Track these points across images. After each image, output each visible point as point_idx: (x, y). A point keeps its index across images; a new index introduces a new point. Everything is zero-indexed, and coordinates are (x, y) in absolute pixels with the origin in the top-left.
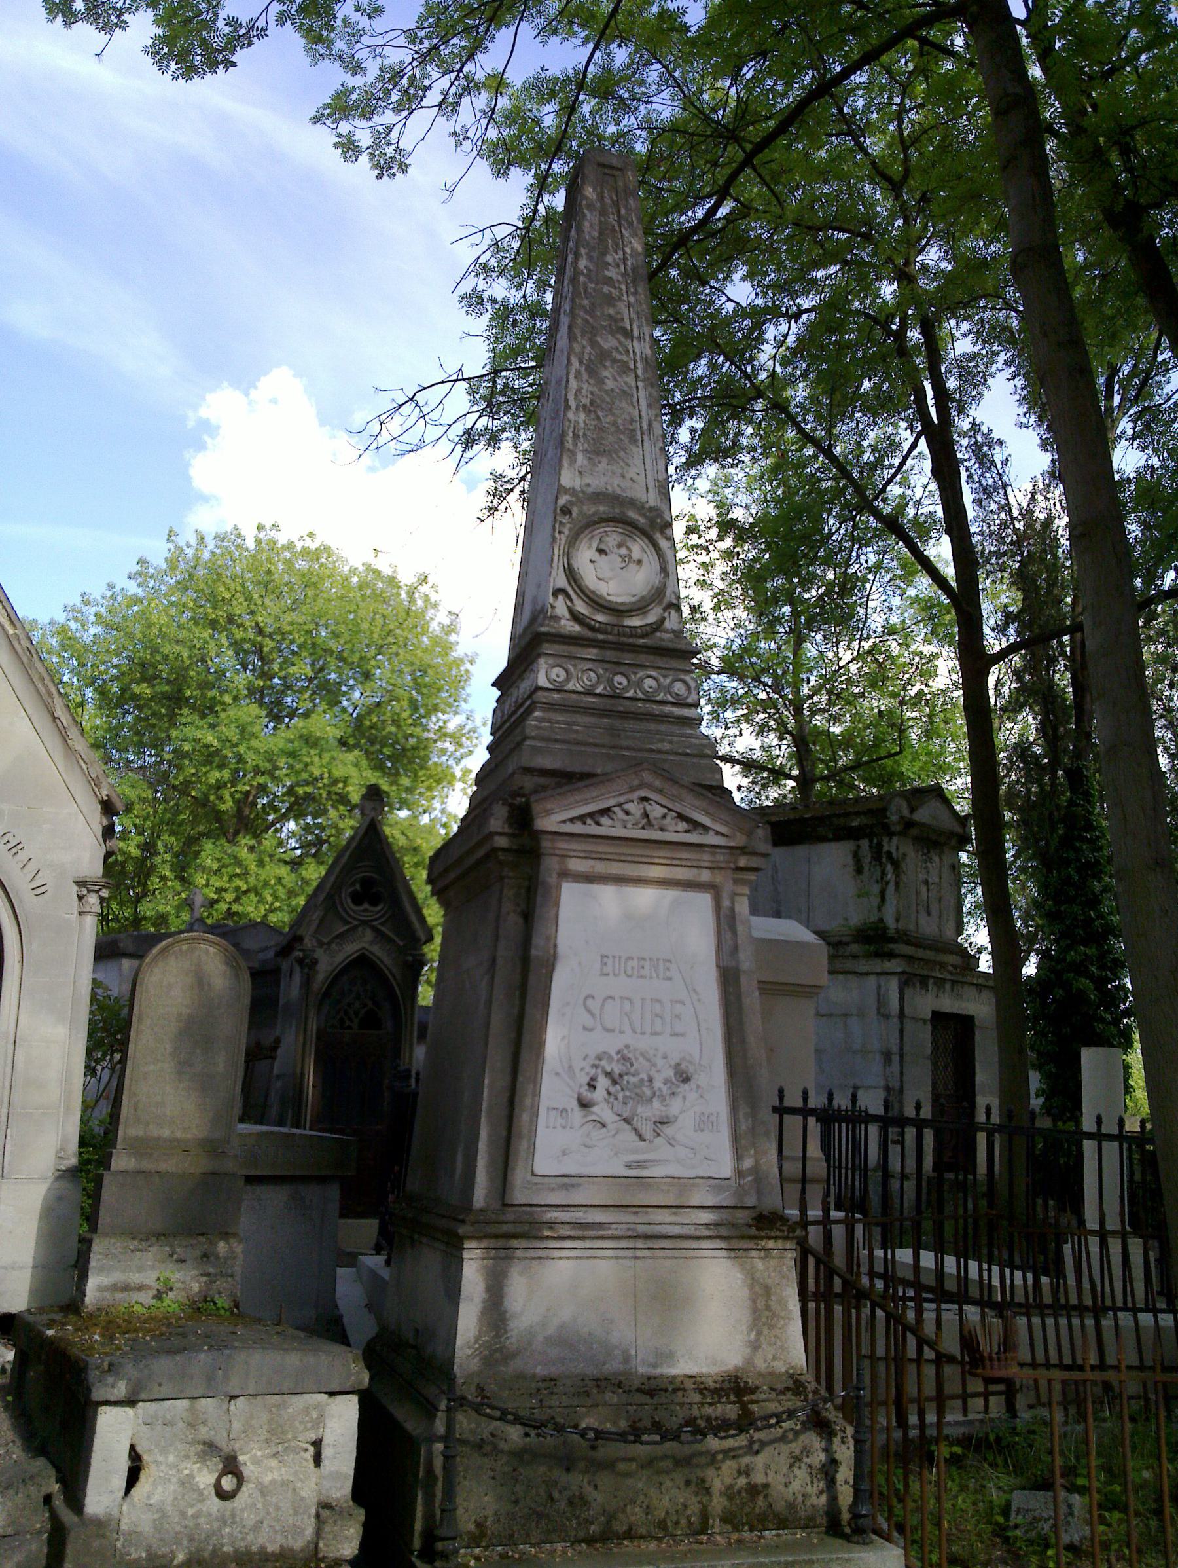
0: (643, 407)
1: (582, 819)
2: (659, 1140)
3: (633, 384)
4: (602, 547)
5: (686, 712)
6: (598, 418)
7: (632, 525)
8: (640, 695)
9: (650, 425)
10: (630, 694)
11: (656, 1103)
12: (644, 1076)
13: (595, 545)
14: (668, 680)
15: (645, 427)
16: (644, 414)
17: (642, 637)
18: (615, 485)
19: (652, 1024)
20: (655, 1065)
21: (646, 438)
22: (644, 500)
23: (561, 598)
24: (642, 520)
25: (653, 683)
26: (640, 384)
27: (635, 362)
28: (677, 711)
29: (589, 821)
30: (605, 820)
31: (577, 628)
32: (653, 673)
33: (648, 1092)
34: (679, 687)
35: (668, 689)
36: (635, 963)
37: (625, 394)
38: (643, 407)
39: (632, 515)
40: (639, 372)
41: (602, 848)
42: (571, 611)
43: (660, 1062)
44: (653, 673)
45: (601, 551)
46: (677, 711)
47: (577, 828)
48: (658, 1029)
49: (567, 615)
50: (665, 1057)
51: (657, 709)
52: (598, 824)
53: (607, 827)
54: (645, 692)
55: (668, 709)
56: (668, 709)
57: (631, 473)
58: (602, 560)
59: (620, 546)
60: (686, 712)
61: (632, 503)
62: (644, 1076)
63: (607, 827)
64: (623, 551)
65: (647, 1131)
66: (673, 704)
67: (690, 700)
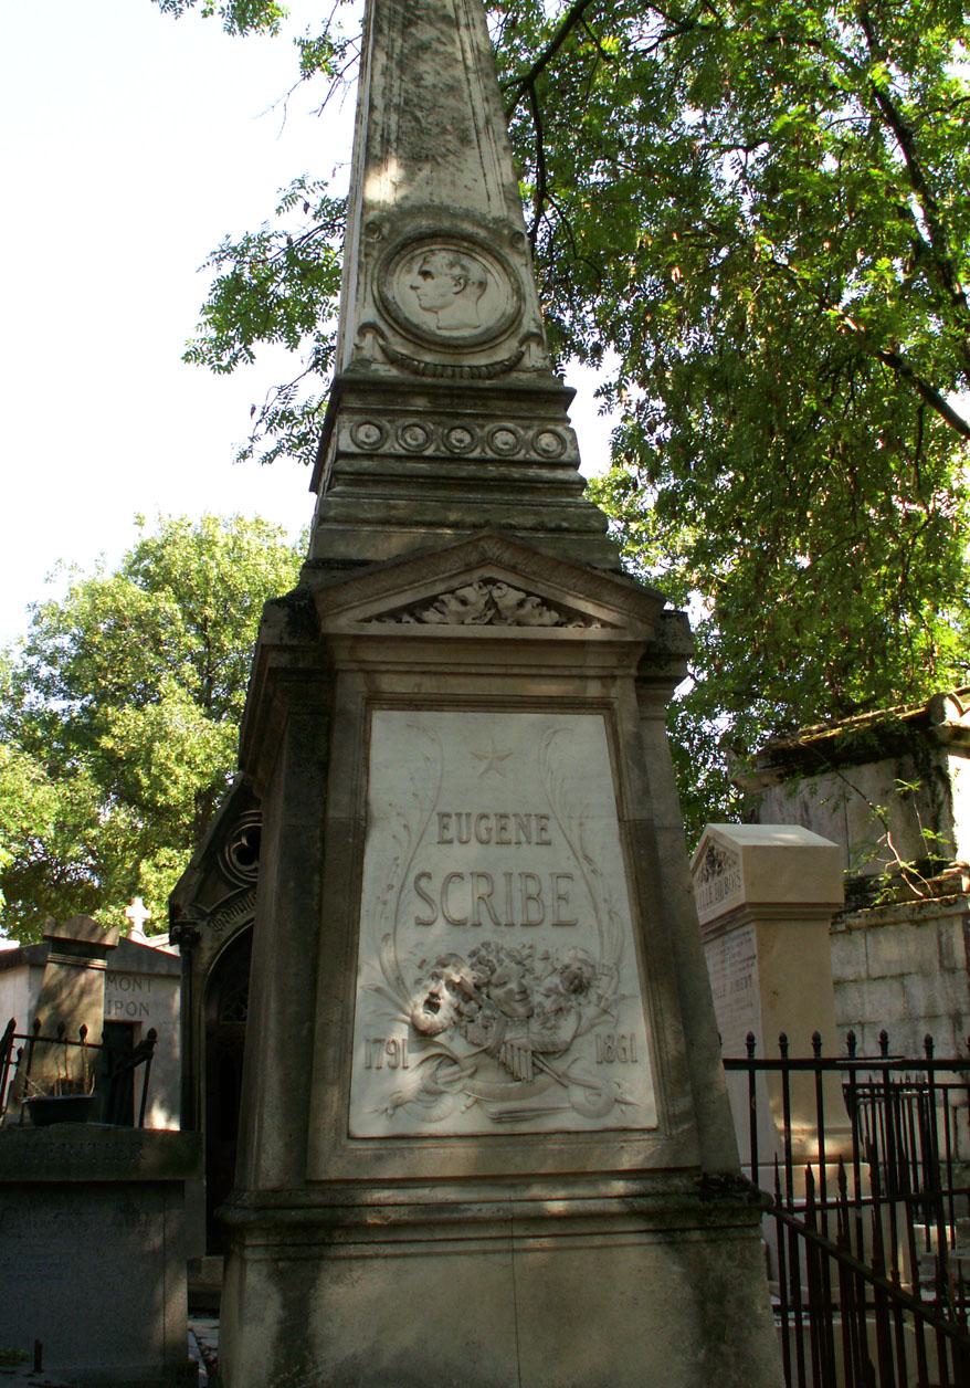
0: (478, 102)
1: (395, 615)
2: (541, 1078)
3: (463, 77)
4: (426, 268)
5: (560, 474)
6: (417, 120)
7: (470, 238)
8: (490, 454)
9: (488, 121)
10: (476, 454)
11: (535, 1025)
12: (513, 986)
13: (416, 268)
14: (531, 433)
15: (481, 123)
16: (478, 110)
17: (489, 377)
18: (443, 196)
19: (525, 909)
20: (531, 971)
21: (483, 136)
22: (484, 209)
23: (369, 337)
24: (482, 233)
25: (510, 438)
26: (472, 76)
27: (463, 51)
28: (546, 473)
29: (406, 618)
30: (430, 615)
31: (394, 372)
32: (510, 425)
33: (521, 1010)
34: (546, 440)
35: (533, 444)
36: (492, 823)
37: (452, 89)
38: (478, 102)
39: (468, 227)
40: (470, 62)
41: (431, 656)
42: (384, 350)
43: (539, 966)
44: (510, 425)
45: (426, 274)
46: (546, 473)
47: (389, 628)
48: (534, 916)
49: (379, 355)
50: (546, 958)
51: (516, 473)
52: (420, 621)
53: (434, 624)
54: (497, 451)
55: (532, 472)
56: (532, 472)
57: (466, 179)
58: (427, 286)
59: (452, 265)
60: (560, 474)
61: (468, 215)
62: (513, 986)
63: (434, 624)
64: (457, 271)
65: (525, 1071)
66: (541, 465)
67: (564, 458)
